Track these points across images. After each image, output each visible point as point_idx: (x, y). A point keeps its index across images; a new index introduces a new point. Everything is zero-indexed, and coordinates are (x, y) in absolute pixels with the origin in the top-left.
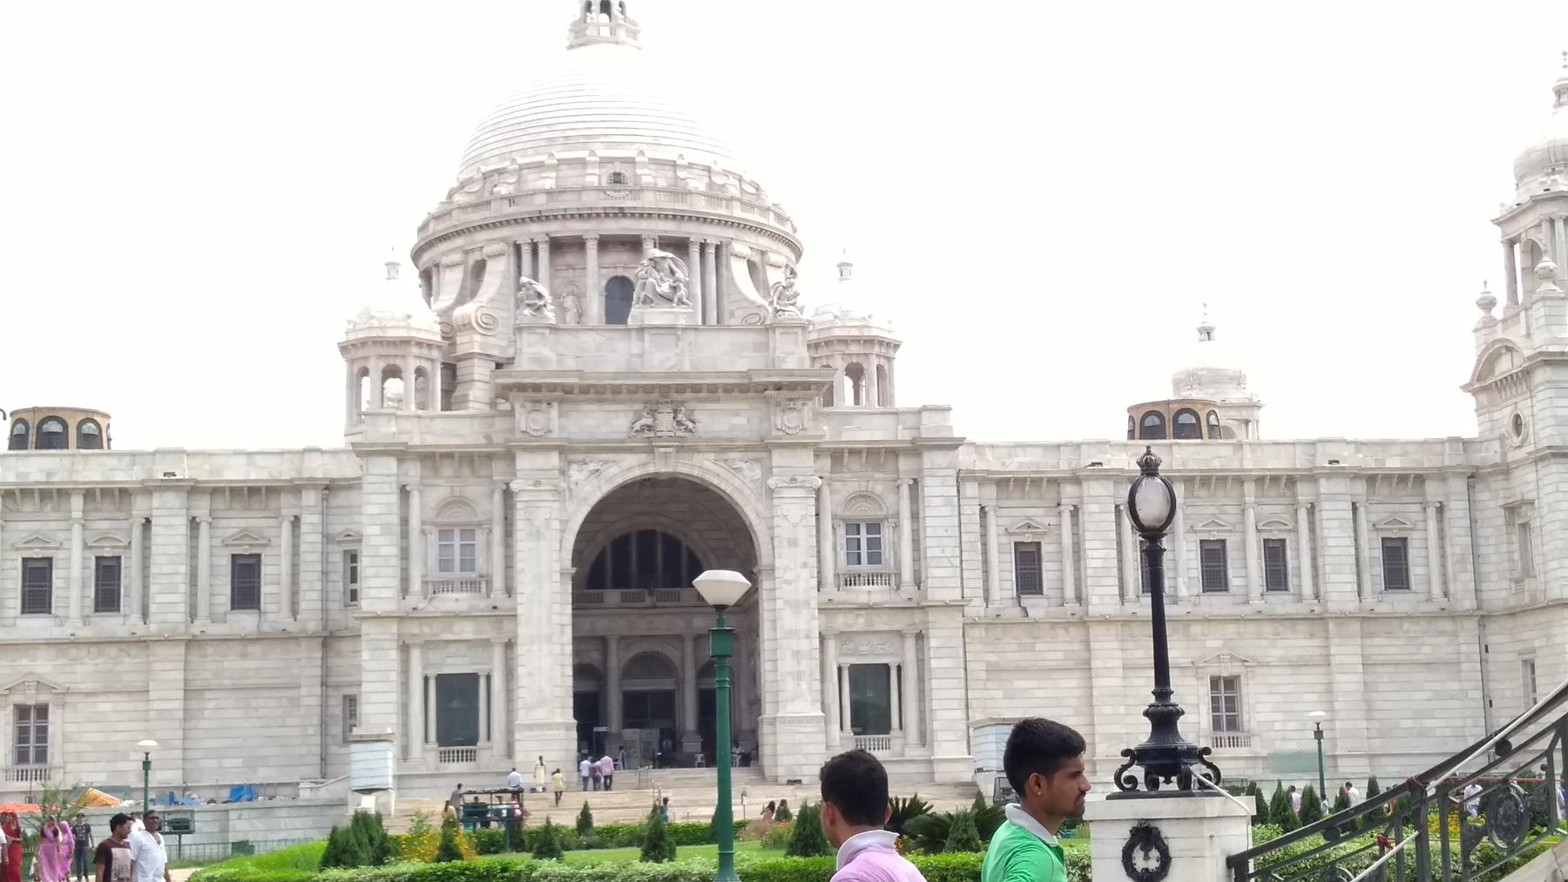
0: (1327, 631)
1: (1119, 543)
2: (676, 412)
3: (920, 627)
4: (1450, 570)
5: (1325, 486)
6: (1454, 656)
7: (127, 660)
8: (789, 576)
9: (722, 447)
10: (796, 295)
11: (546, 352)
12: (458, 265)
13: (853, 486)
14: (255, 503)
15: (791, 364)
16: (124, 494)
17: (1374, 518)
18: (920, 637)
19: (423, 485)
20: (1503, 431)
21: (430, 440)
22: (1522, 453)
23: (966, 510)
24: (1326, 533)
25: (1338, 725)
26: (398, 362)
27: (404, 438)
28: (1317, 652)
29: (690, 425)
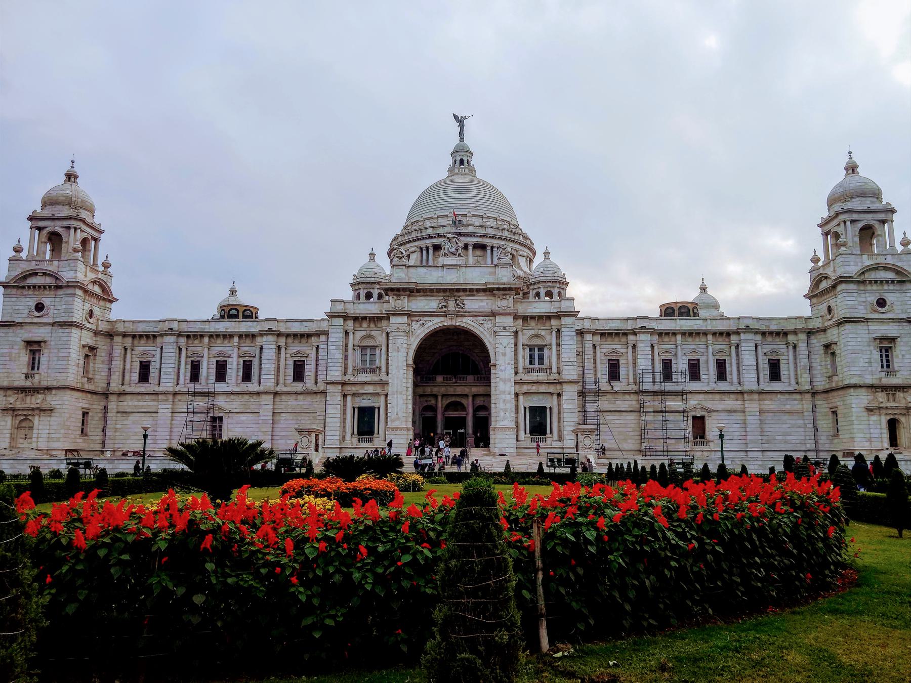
0: (744, 398)
1: (653, 360)
2: (456, 300)
3: (560, 391)
4: (799, 372)
5: (743, 336)
6: (801, 409)
7: (252, 400)
8: (502, 368)
9: (475, 315)
11: (403, 275)
13: (532, 332)
14: (304, 340)
15: (505, 280)
16: (254, 336)
17: (765, 351)
18: (559, 395)
19: (354, 331)
20: (823, 313)
21: (358, 312)
22: (832, 322)
23: (586, 345)
24: (743, 356)
25: (748, 437)
26: (371, 290)
27: (348, 311)
28: (739, 406)
29: (462, 306)
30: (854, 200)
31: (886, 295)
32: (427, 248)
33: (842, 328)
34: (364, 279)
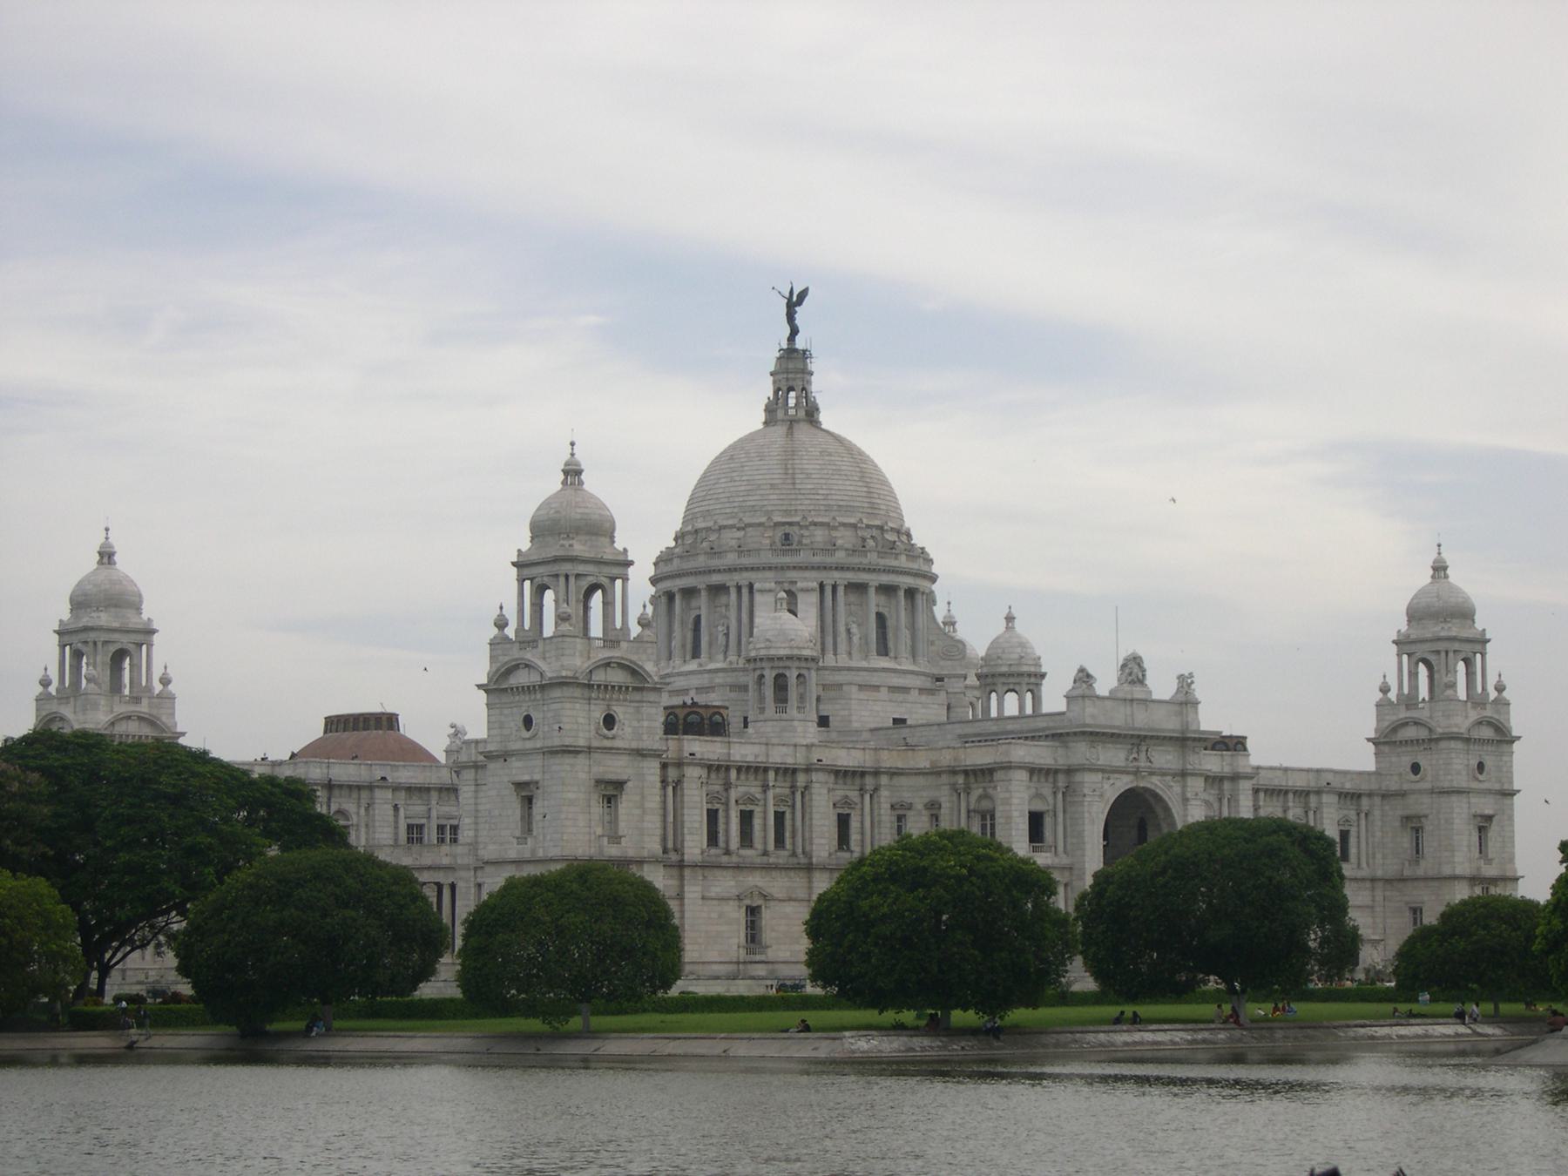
5: (1326, 798)
9: (1163, 774)
10: (1192, 682)
12: (770, 591)
14: (849, 781)
16: (795, 771)
22: (1426, 785)
26: (803, 672)
30: (1454, 621)
31: (1487, 757)
32: (834, 588)
33: (1444, 799)
34: (796, 652)
